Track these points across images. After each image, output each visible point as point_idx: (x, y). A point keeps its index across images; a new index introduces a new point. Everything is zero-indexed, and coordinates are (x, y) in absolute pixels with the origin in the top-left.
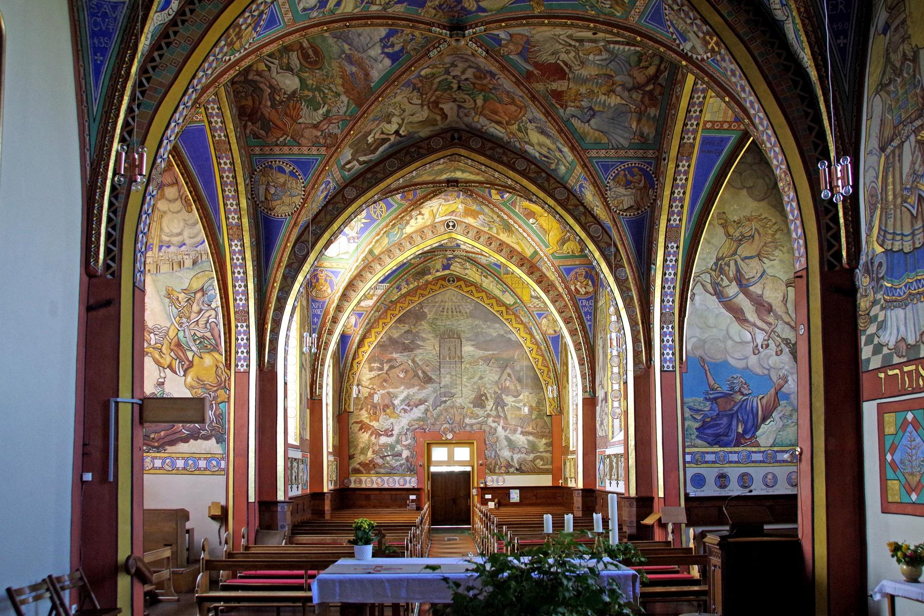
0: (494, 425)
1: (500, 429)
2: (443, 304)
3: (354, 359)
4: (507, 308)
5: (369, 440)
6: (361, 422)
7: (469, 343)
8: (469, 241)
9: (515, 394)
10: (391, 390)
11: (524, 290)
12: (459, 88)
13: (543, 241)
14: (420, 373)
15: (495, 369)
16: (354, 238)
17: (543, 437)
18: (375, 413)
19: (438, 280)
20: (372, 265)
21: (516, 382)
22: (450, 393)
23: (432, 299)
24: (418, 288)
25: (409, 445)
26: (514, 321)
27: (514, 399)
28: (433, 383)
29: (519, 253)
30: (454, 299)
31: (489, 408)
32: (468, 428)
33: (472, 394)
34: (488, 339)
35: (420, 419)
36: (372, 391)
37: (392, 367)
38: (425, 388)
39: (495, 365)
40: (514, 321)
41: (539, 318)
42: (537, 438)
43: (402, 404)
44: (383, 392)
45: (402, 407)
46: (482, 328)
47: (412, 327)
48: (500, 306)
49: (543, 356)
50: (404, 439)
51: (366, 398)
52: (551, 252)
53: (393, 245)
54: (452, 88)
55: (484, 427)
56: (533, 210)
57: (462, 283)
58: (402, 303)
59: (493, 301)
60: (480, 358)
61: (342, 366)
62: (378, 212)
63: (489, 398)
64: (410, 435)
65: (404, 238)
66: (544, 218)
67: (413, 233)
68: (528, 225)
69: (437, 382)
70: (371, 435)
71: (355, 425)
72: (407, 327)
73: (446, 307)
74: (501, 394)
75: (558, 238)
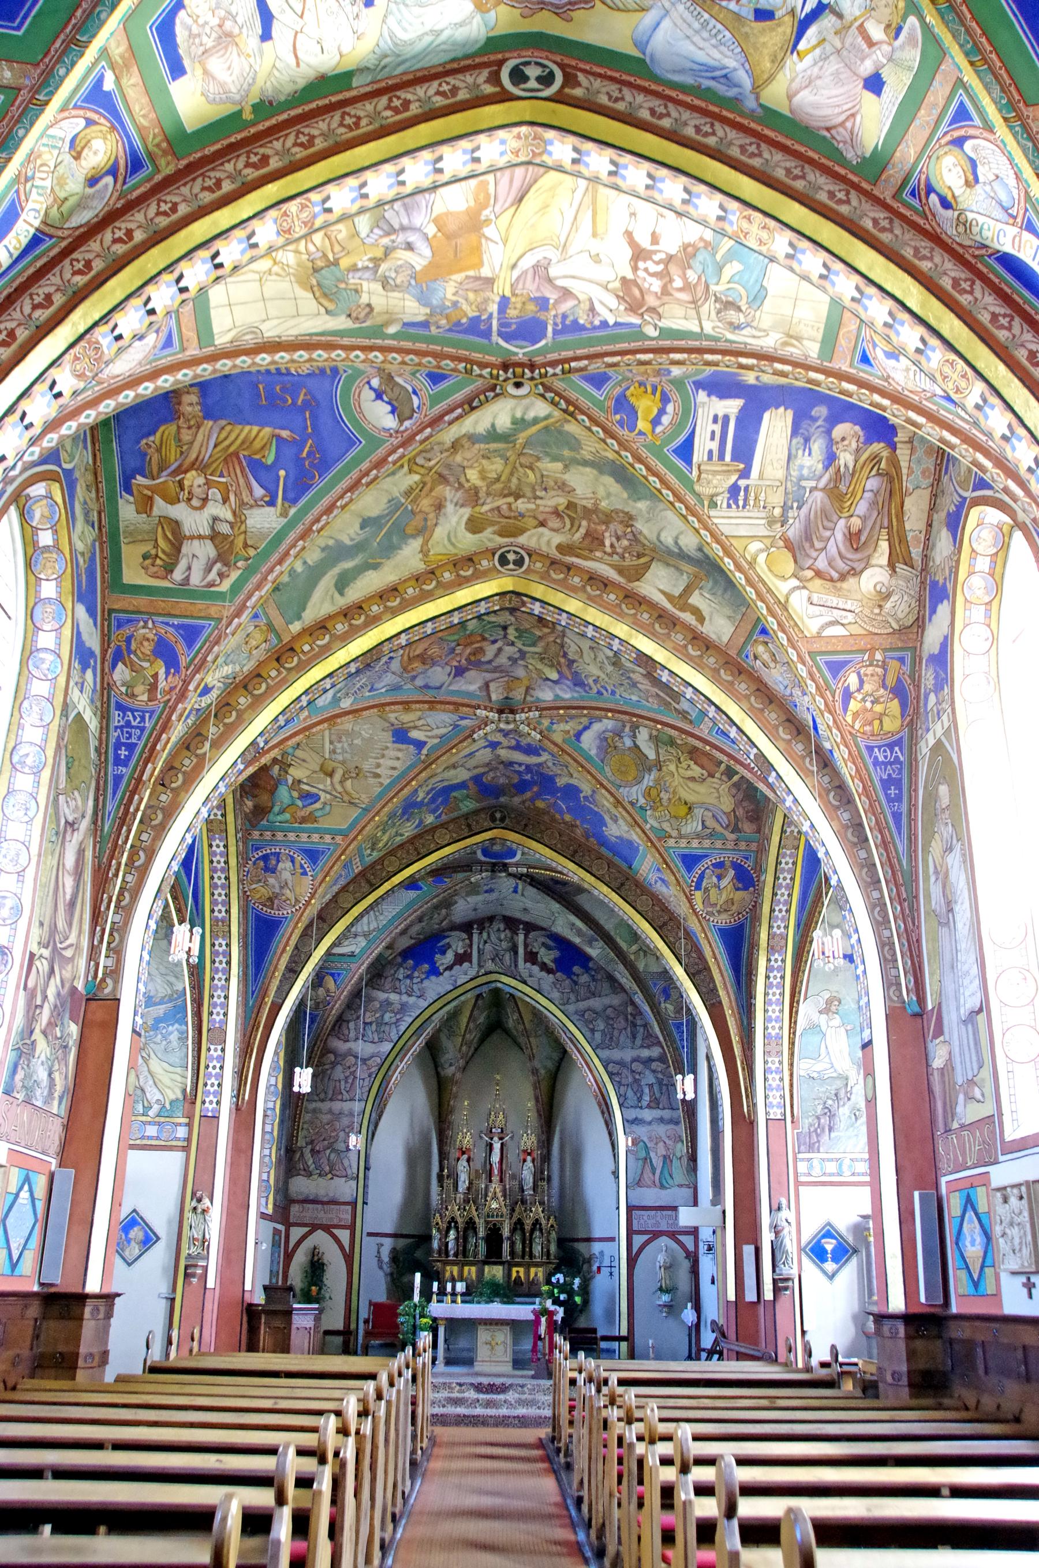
12: (505, 628)
54: (516, 630)
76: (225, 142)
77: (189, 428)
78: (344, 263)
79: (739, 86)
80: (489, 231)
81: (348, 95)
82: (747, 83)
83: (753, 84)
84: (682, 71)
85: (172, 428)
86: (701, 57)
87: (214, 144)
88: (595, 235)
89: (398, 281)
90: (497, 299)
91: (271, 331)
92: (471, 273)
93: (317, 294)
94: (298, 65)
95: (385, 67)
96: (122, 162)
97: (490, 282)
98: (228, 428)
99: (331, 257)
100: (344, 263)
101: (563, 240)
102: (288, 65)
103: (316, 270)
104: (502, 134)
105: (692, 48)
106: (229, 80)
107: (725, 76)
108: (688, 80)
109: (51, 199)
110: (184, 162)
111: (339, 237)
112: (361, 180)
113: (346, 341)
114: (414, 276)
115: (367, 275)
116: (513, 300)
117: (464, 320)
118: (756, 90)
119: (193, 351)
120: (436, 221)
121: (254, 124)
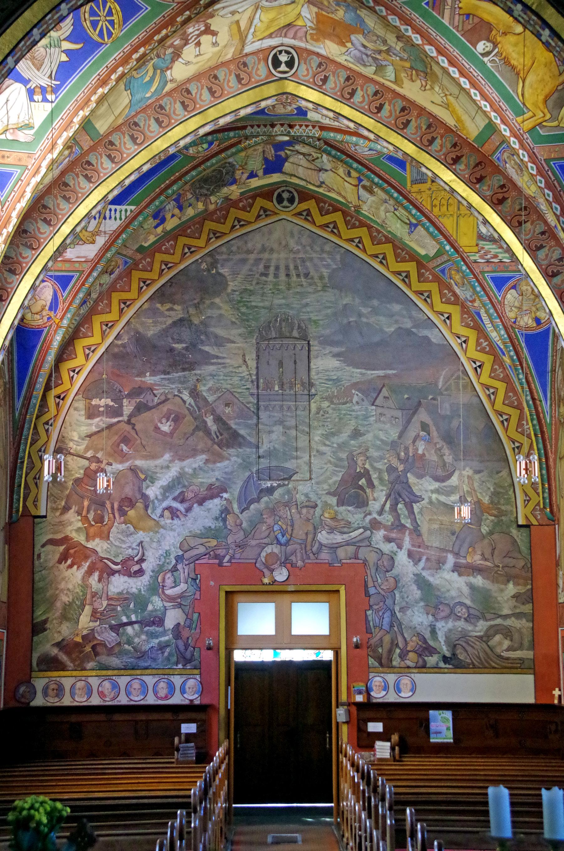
0: (387, 548)
1: (402, 557)
2: (266, 256)
3: (48, 388)
4: (420, 265)
5: (85, 586)
6: (66, 539)
7: (328, 349)
8: (328, 102)
9: (440, 472)
10: (139, 463)
11: (462, 221)
13: (508, 99)
14: (209, 420)
15: (389, 413)
16: (43, 90)
17: (508, 578)
18: (100, 520)
19: (254, 198)
20: (92, 158)
21: (441, 444)
22: (283, 469)
23: (240, 243)
24: (206, 216)
25: (181, 596)
26: (436, 298)
27: (436, 485)
28: (240, 445)
29: (448, 129)
30: (292, 243)
31: (375, 506)
32: (325, 556)
33: (334, 473)
34: (376, 339)
35: (208, 533)
36: (94, 466)
37: (141, 408)
38: (221, 458)
39: (390, 403)
40: (436, 298)
41: (499, 289)
42: (495, 580)
43: (165, 498)
44: (120, 467)
45: (165, 504)
46: (360, 315)
47: (192, 311)
48: (403, 261)
49: (507, 380)
50: (169, 581)
51: (77, 481)
52: (528, 125)
53: (144, 110)
55: (363, 553)
56: (486, 17)
57: (311, 205)
58: (167, 252)
59: (387, 249)
60: (355, 385)
61: (18, 405)
62: (103, 24)
63: (376, 482)
64: (183, 571)
65: (169, 94)
66: (511, 39)
67: (189, 80)
68: (472, 57)
69: (250, 445)
70: (90, 572)
71: (49, 547)
72: (178, 312)
73: (273, 264)
74: (405, 472)
75: (547, 90)
78: (408, 65)
80: (309, 24)
88: (238, 22)
89: (375, 38)
100: (408, 65)
103: (426, 74)
115: (395, 52)
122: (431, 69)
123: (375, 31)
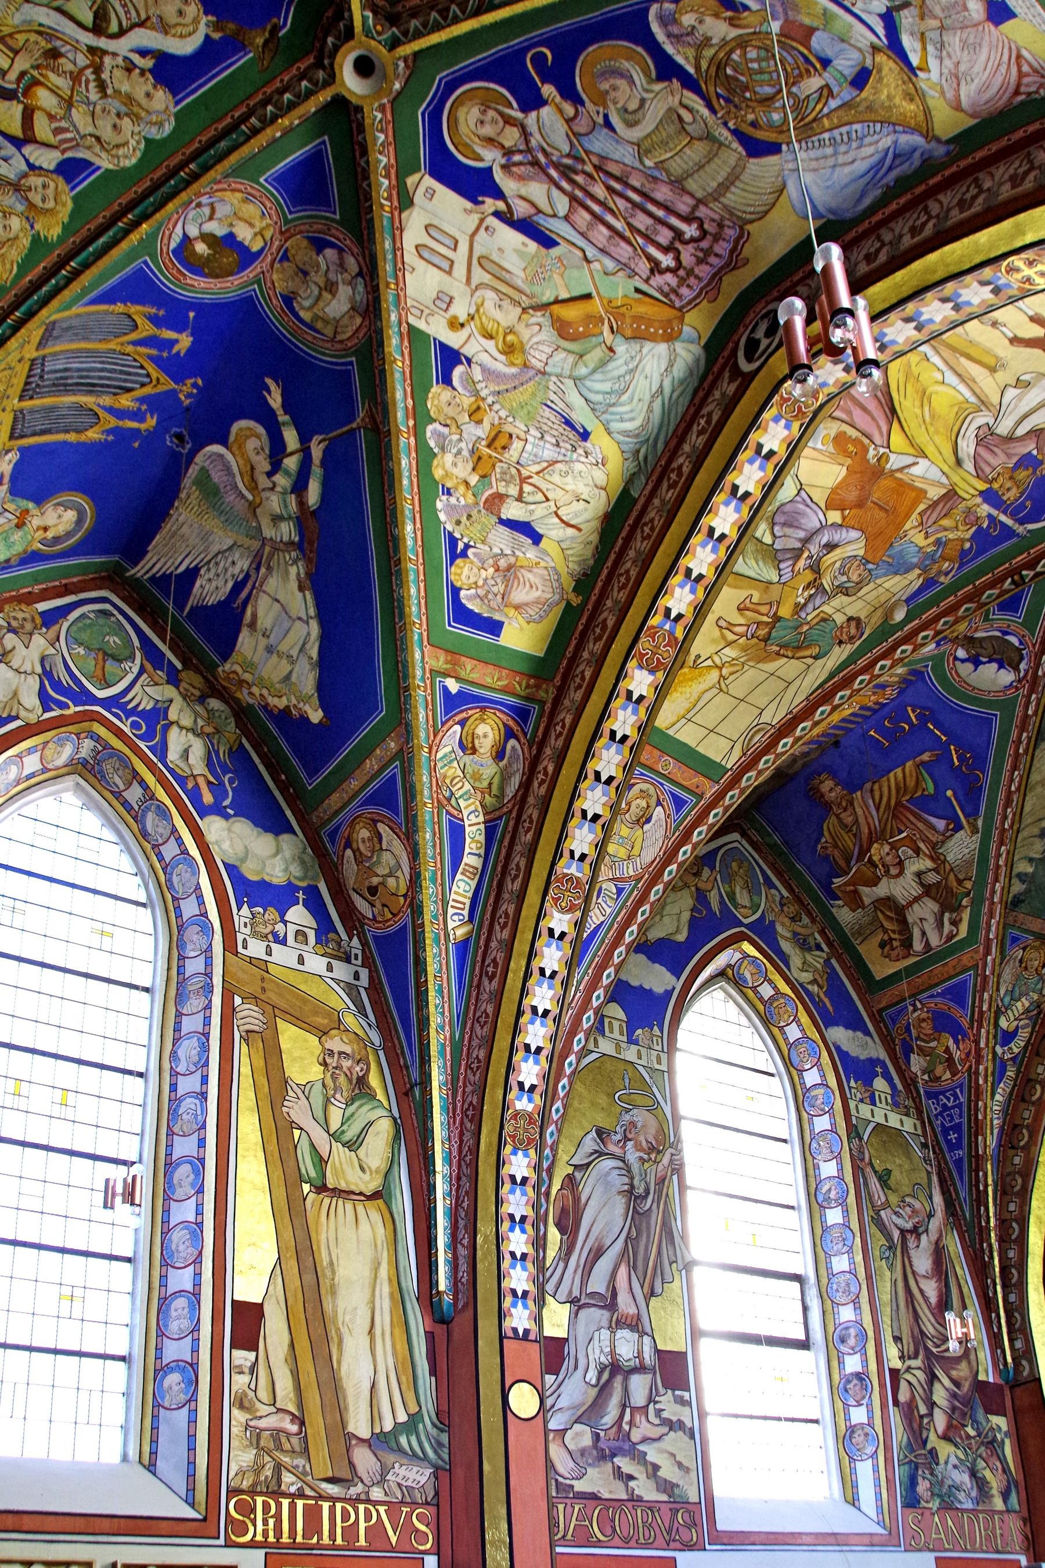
76: (577, 635)
77: (845, 810)
78: (785, 612)
79: (915, 150)
80: (895, 462)
81: (638, 507)
82: (917, 140)
83: (921, 135)
84: (863, 194)
85: (833, 819)
86: (861, 166)
87: (569, 644)
88: (993, 370)
89: (855, 578)
90: (979, 500)
91: (774, 716)
92: (922, 507)
93: (790, 654)
94: (579, 530)
95: (646, 458)
96: (511, 723)
97: (951, 495)
98: (876, 787)
99: (765, 619)
100: (785, 612)
101: (973, 399)
102: (573, 538)
103: (766, 640)
104: (767, 415)
105: (847, 170)
106: (538, 593)
107: (896, 156)
108: (876, 193)
109: (479, 794)
110: (558, 678)
111: (755, 600)
112: (682, 571)
113: (862, 663)
114: (865, 561)
116: (996, 486)
117: (967, 545)
118: (928, 134)
119: (710, 790)
120: (830, 505)
121: (585, 602)
122: (778, 654)
123: (872, 586)
